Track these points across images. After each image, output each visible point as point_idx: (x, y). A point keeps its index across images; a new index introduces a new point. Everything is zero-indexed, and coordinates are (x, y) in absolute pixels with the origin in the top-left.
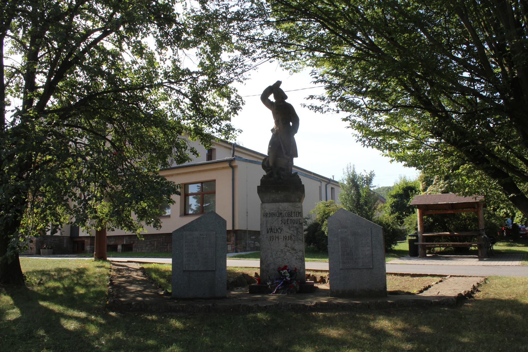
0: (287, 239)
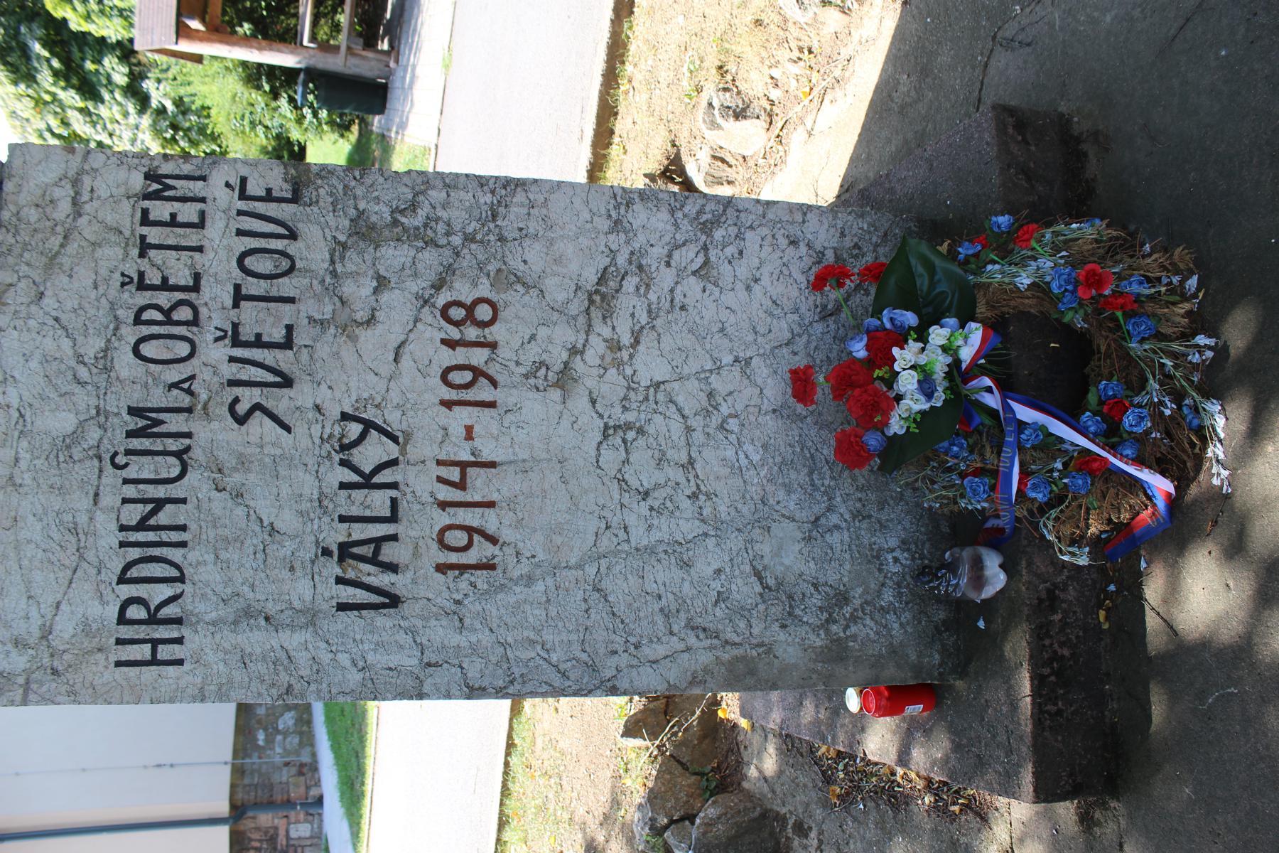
0: (478, 357)
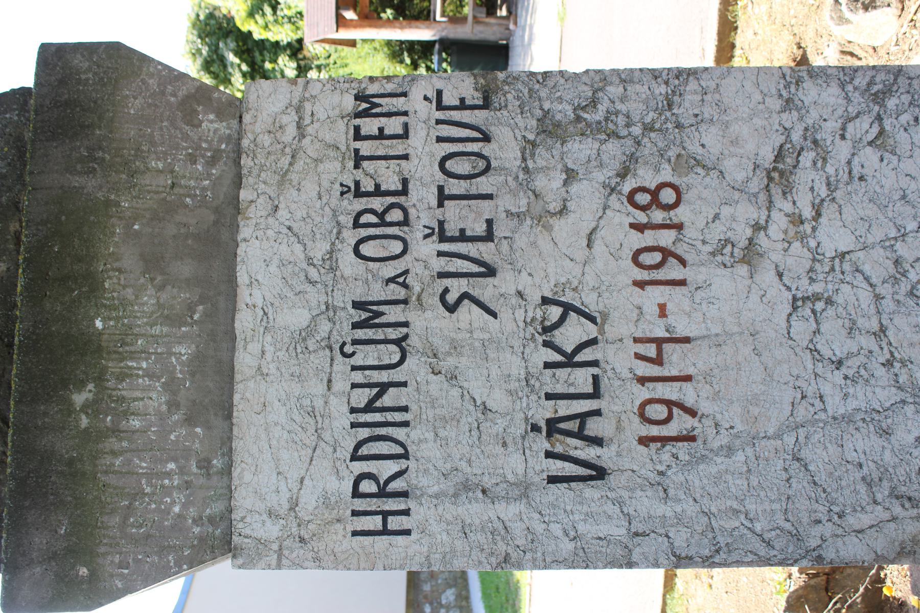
0: (666, 238)
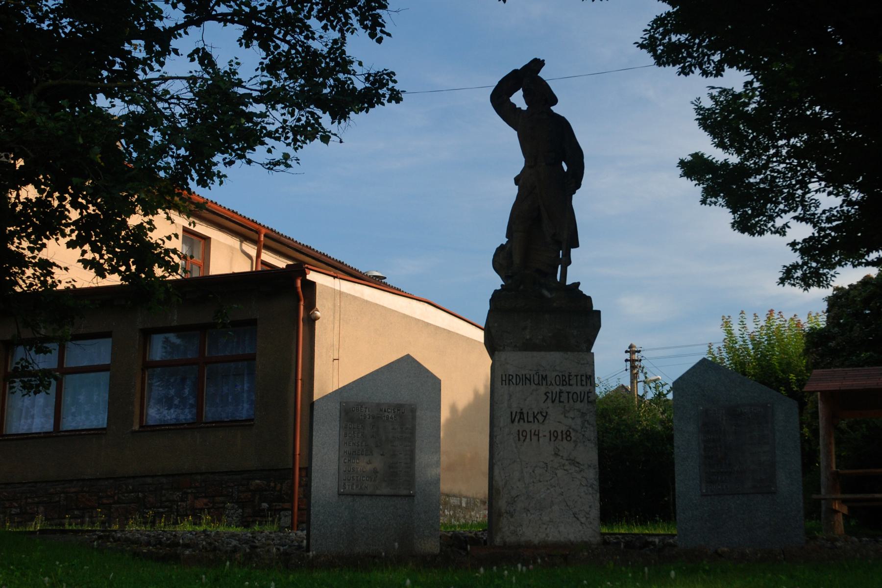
0: (560, 437)
